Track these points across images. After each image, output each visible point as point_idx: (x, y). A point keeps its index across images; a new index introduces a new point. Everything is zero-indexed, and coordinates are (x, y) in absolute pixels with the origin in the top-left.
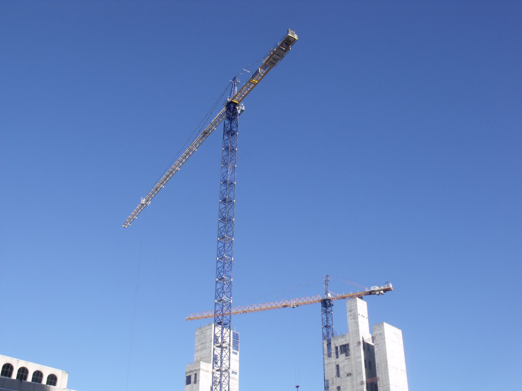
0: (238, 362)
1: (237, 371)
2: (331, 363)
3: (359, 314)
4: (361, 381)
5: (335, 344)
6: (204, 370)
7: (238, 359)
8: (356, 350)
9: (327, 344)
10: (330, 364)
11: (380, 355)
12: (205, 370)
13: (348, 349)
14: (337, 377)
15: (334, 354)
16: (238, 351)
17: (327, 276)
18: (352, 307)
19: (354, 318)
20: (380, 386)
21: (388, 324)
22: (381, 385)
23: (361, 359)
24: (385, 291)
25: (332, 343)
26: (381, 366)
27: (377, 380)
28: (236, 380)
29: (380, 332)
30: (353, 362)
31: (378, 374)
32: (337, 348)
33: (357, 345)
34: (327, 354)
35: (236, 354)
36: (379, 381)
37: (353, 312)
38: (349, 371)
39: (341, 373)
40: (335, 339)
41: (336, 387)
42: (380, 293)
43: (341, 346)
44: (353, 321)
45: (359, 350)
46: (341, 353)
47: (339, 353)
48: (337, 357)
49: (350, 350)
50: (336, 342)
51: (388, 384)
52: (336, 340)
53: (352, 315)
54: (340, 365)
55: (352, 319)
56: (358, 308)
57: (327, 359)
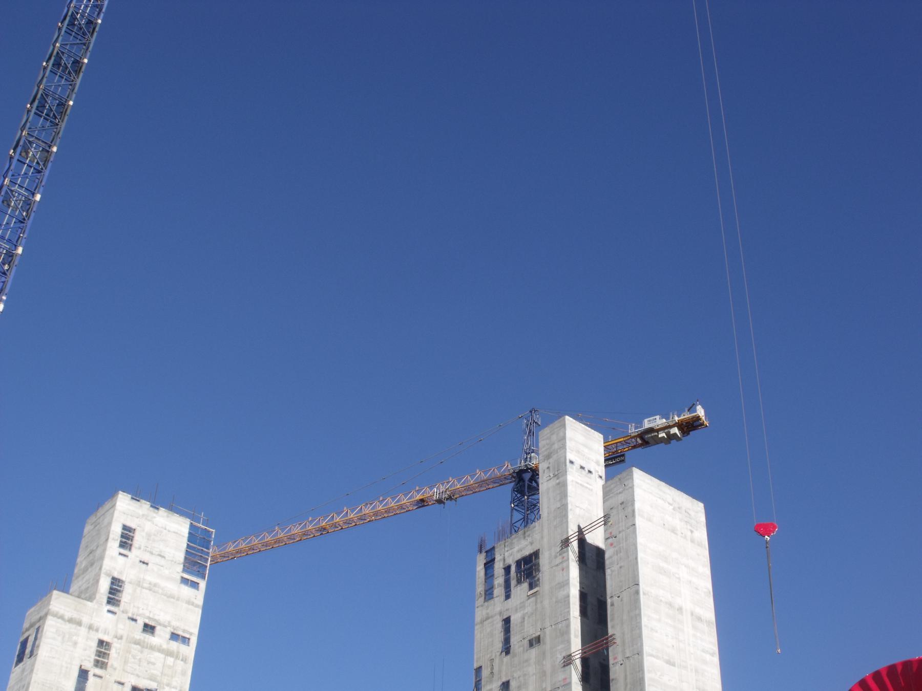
0: (200, 611)
1: (191, 634)
2: (492, 617)
3: (572, 462)
4: (564, 654)
5: (504, 560)
6: (62, 617)
7: (200, 600)
8: (557, 565)
9: (485, 564)
10: (487, 618)
11: (619, 565)
12: (66, 618)
13: (537, 567)
14: (504, 653)
15: (500, 588)
16: (203, 577)
17: (531, 412)
18: (554, 444)
19: (556, 473)
20: (616, 661)
21: (646, 472)
22: (620, 658)
23: (569, 588)
24: (682, 426)
25: (498, 557)
26: (622, 600)
27: (607, 643)
28: (184, 660)
29: (621, 498)
30: (546, 603)
31: (613, 627)
32: (507, 569)
33: (558, 549)
34: (483, 593)
35: (195, 585)
36: (615, 645)
37: (555, 457)
38: (533, 632)
39: (514, 640)
40: (505, 545)
41: (500, 683)
42: (668, 434)
43: (518, 563)
44: (554, 482)
45: (565, 565)
46: (519, 582)
47: (513, 582)
48: (508, 597)
49: (541, 568)
50: (506, 554)
51: (640, 653)
52: (506, 549)
53: (551, 469)
54: (512, 619)
55: (550, 479)
56: (569, 444)
57: (482, 606)
